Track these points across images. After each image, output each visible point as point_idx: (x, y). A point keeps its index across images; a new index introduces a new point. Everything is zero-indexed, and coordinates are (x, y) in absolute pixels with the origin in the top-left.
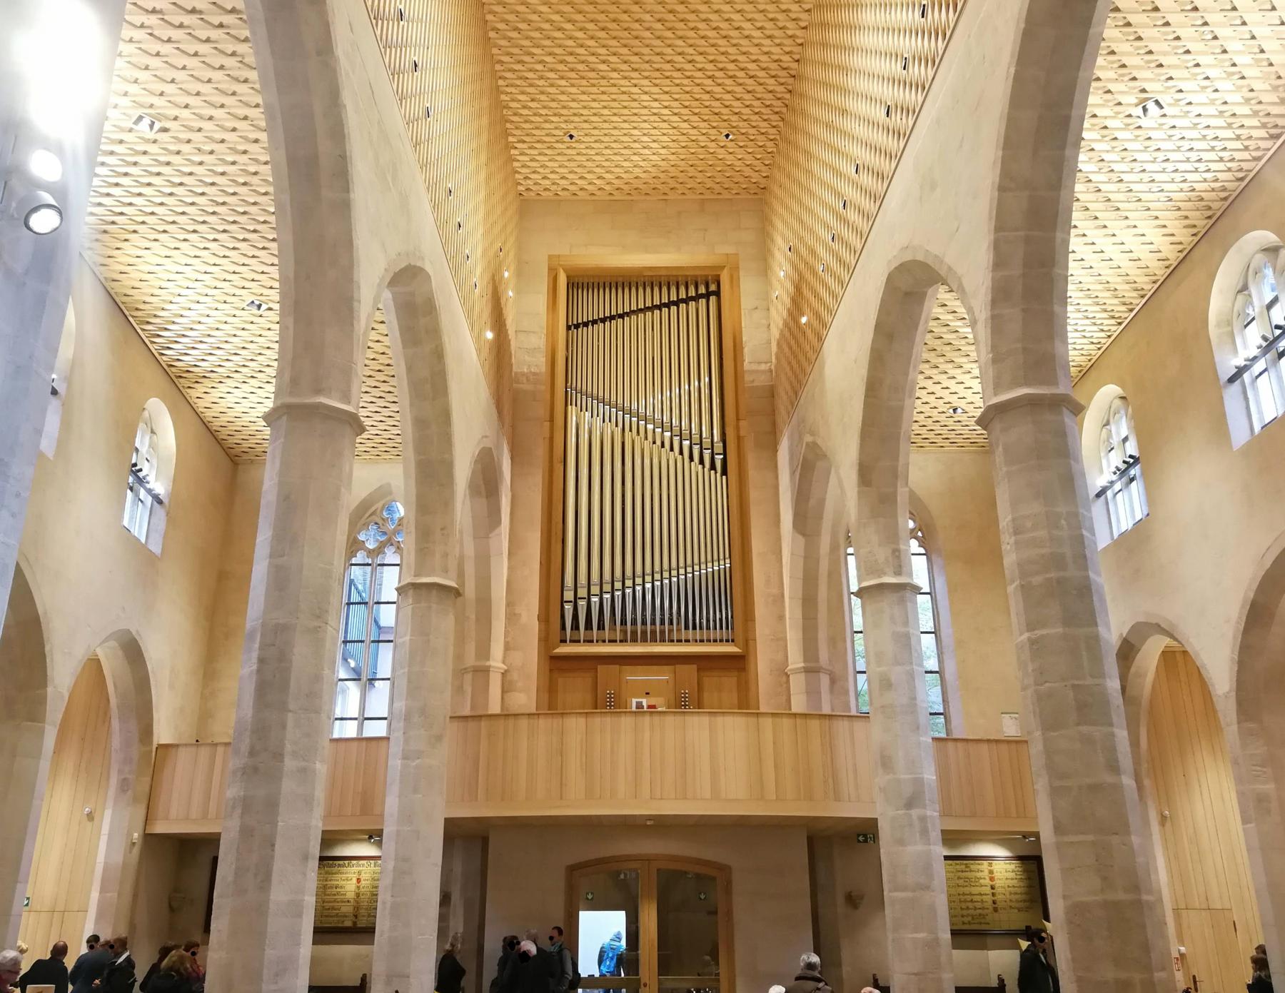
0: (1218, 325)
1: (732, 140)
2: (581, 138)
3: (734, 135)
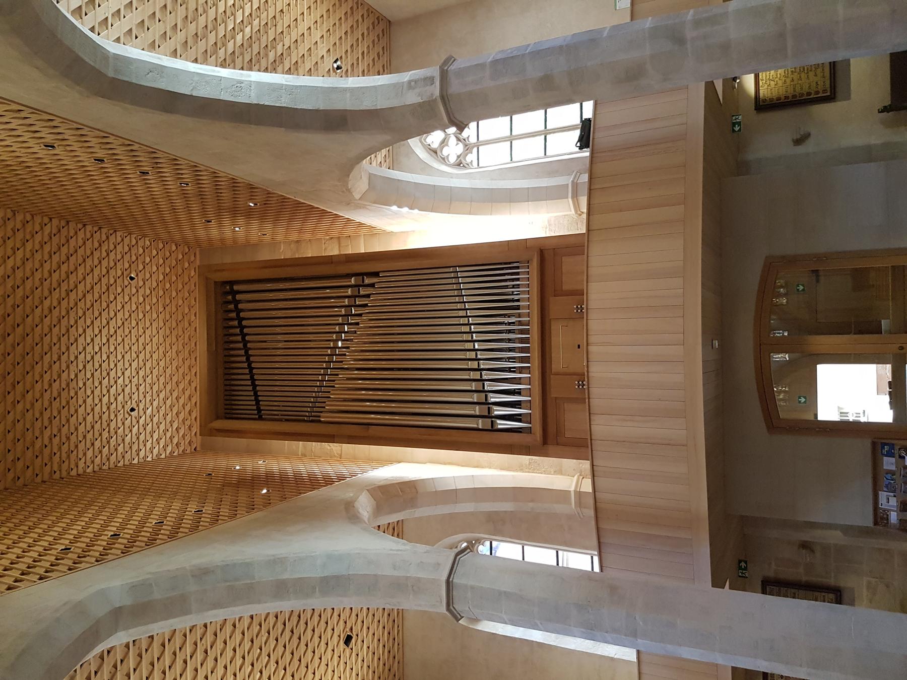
1: (137, 275)
3: (131, 273)
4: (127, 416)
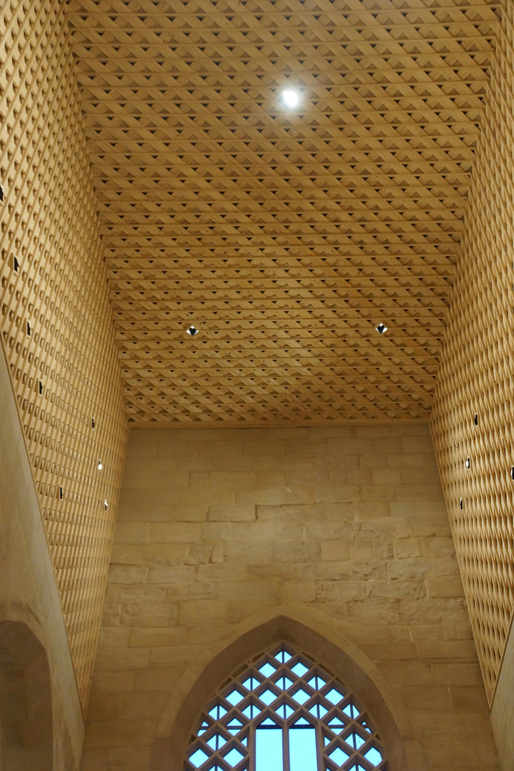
1: (386, 335)
2: (204, 333)
3: (389, 327)
4: (184, 323)
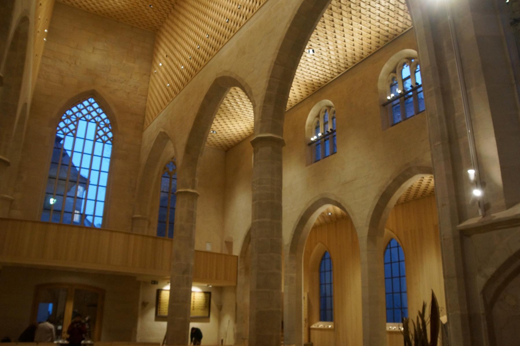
0: (308, 126)
1: (152, 8)
3: (153, 6)
